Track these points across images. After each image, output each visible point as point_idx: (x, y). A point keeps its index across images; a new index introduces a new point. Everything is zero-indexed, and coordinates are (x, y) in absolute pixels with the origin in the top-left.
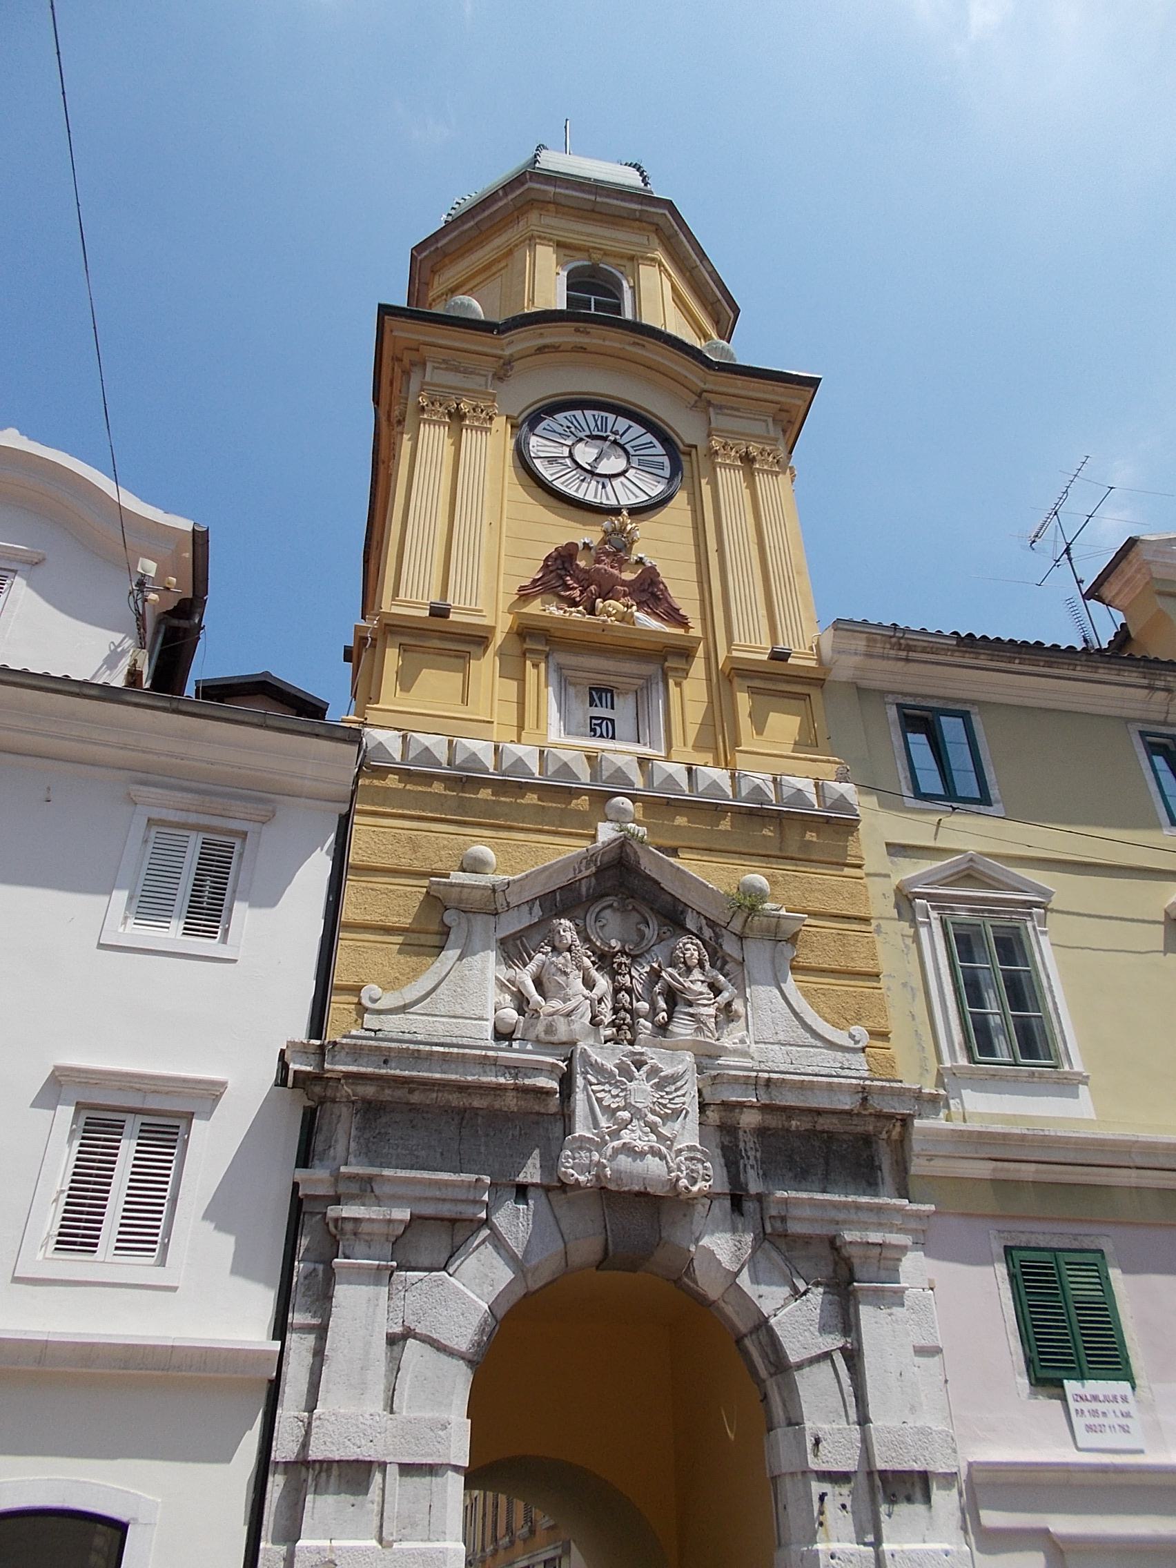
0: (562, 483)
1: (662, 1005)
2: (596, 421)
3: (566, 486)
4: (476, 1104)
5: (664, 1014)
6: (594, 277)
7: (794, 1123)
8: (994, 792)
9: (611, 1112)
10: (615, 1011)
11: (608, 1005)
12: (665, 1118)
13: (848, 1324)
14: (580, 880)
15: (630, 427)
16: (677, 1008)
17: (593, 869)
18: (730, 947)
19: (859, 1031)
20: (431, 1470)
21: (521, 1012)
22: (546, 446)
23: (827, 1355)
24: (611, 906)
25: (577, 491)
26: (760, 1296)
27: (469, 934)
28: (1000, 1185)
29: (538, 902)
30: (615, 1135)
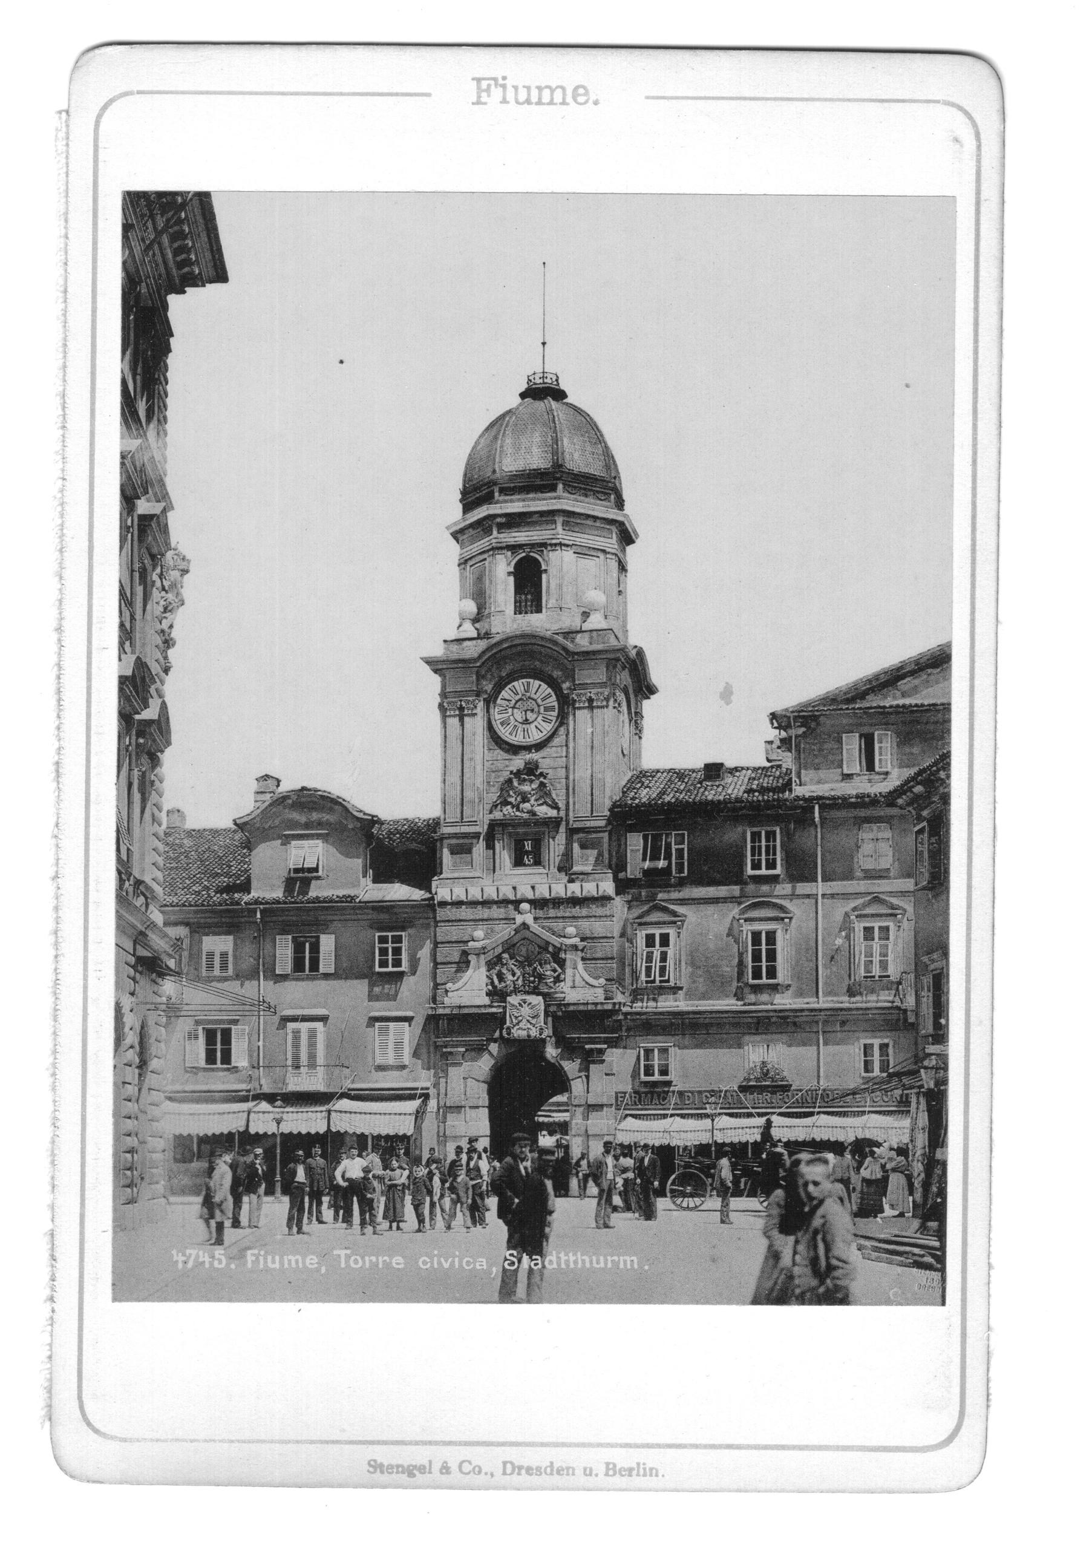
9: (516, 1017)
10: (524, 981)
12: (533, 1018)
19: (602, 981)
20: (477, 1107)
23: (580, 1077)
30: (518, 1024)
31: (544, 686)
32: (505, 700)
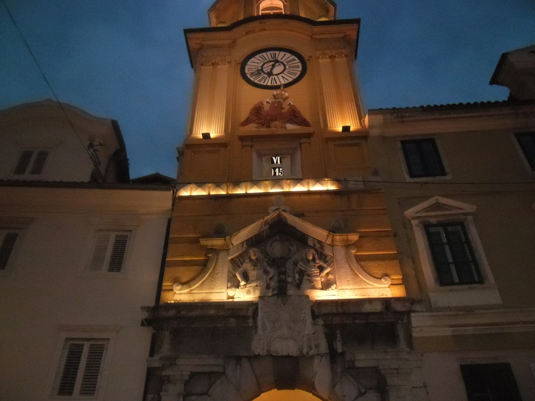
0: (258, 81)
1: (297, 276)
3: (260, 82)
4: (219, 325)
5: (298, 281)
6: (272, 4)
7: (357, 321)
8: (447, 169)
11: (276, 278)
14: (263, 231)
15: (285, 55)
16: (304, 278)
17: (268, 226)
22: (251, 68)
24: (276, 240)
25: (264, 83)
26: (344, 396)
27: (217, 259)
29: (245, 243)
32: (255, 63)
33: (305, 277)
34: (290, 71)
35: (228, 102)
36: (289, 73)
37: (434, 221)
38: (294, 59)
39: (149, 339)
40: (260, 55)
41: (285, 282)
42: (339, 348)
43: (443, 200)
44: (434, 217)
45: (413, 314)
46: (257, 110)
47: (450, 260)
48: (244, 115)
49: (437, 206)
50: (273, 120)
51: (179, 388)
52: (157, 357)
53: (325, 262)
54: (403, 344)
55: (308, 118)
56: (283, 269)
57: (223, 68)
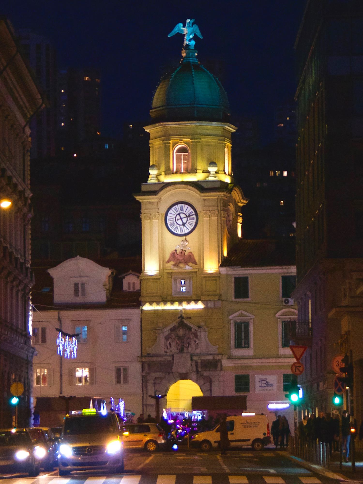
1: (187, 345)
2: (180, 207)
8: (250, 295)
13: (211, 387)
17: (177, 323)
18: (198, 334)
21: (167, 348)
22: (170, 219)
28: (235, 367)
31: (189, 208)
32: (172, 214)
33: (190, 346)
34: (190, 222)
35: (159, 247)
36: (189, 224)
37: (239, 321)
38: (192, 211)
39: (141, 366)
40: (174, 207)
41: (184, 346)
42: (200, 369)
43: (244, 312)
44: (239, 320)
45: (222, 360)
46: (174, 254)
47: (243, 337)
48: (167, 256)
49: (242, 315)
50: (180, 262)
51: (153, 382)
52: (144, 372)
53: (197, 338)
54: (219, 369)
55: (197, 259)
56: (183, 341)
57: (155, 221)
